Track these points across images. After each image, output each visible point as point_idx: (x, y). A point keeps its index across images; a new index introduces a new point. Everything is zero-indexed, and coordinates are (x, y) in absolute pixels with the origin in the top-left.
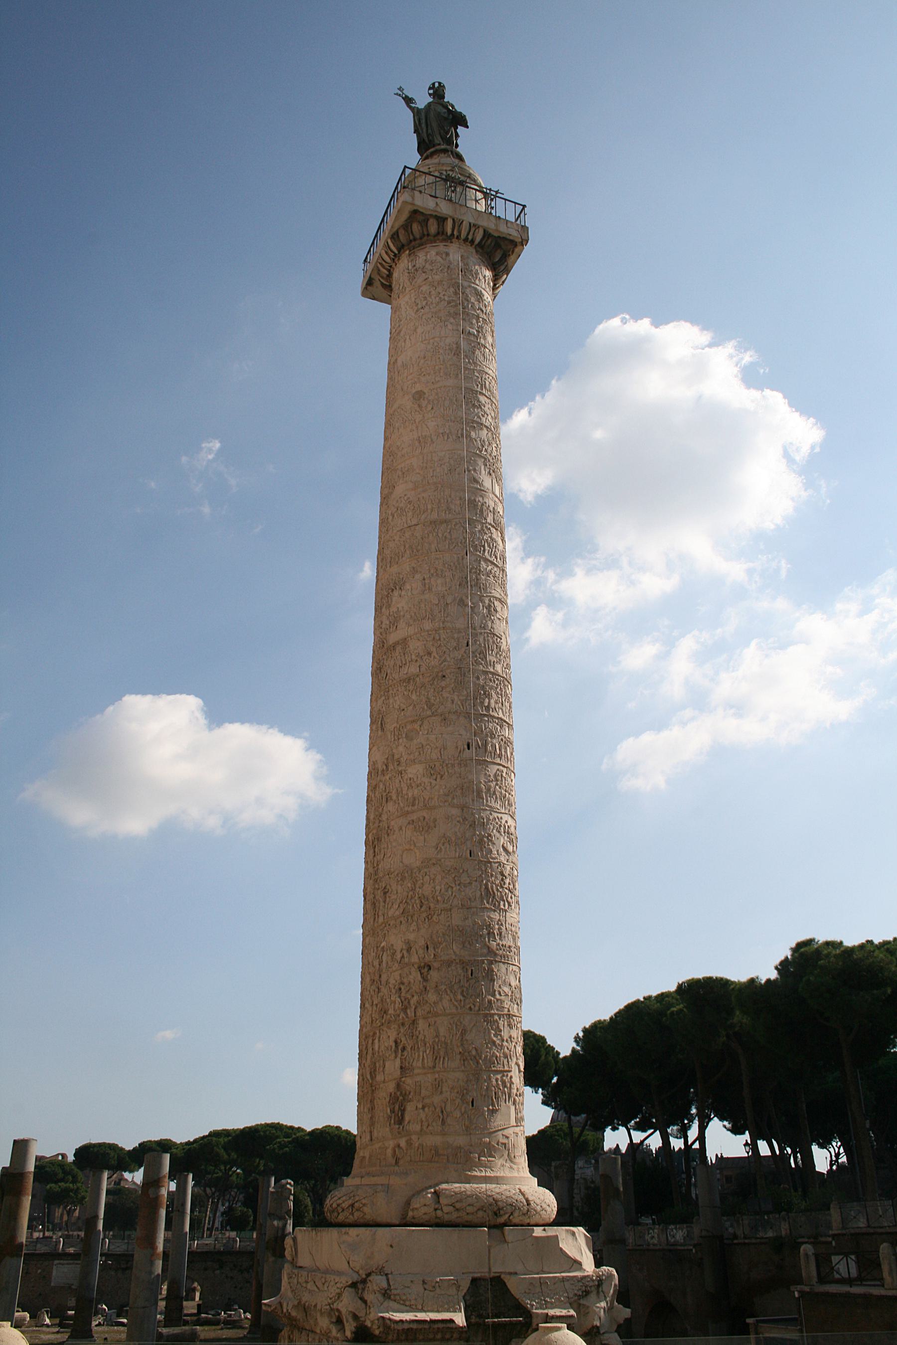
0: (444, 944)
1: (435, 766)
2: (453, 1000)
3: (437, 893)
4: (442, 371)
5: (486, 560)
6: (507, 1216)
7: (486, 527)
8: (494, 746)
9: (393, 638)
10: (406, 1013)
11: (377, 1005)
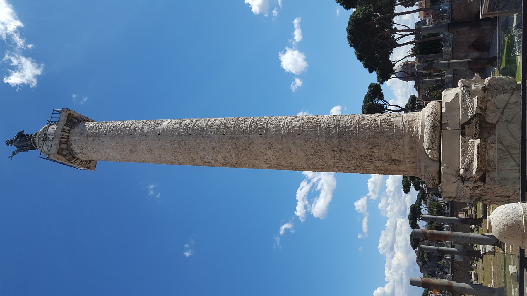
0: (332, 144)
2: (353, 141)
3: (314, 147)
4: (121, 143)
5: (193, 127)
6: (437, 122)
7: (181, 127)
8: (260, 125)
9: (222, 161)
10: (358, 159)
11: (355, 168)
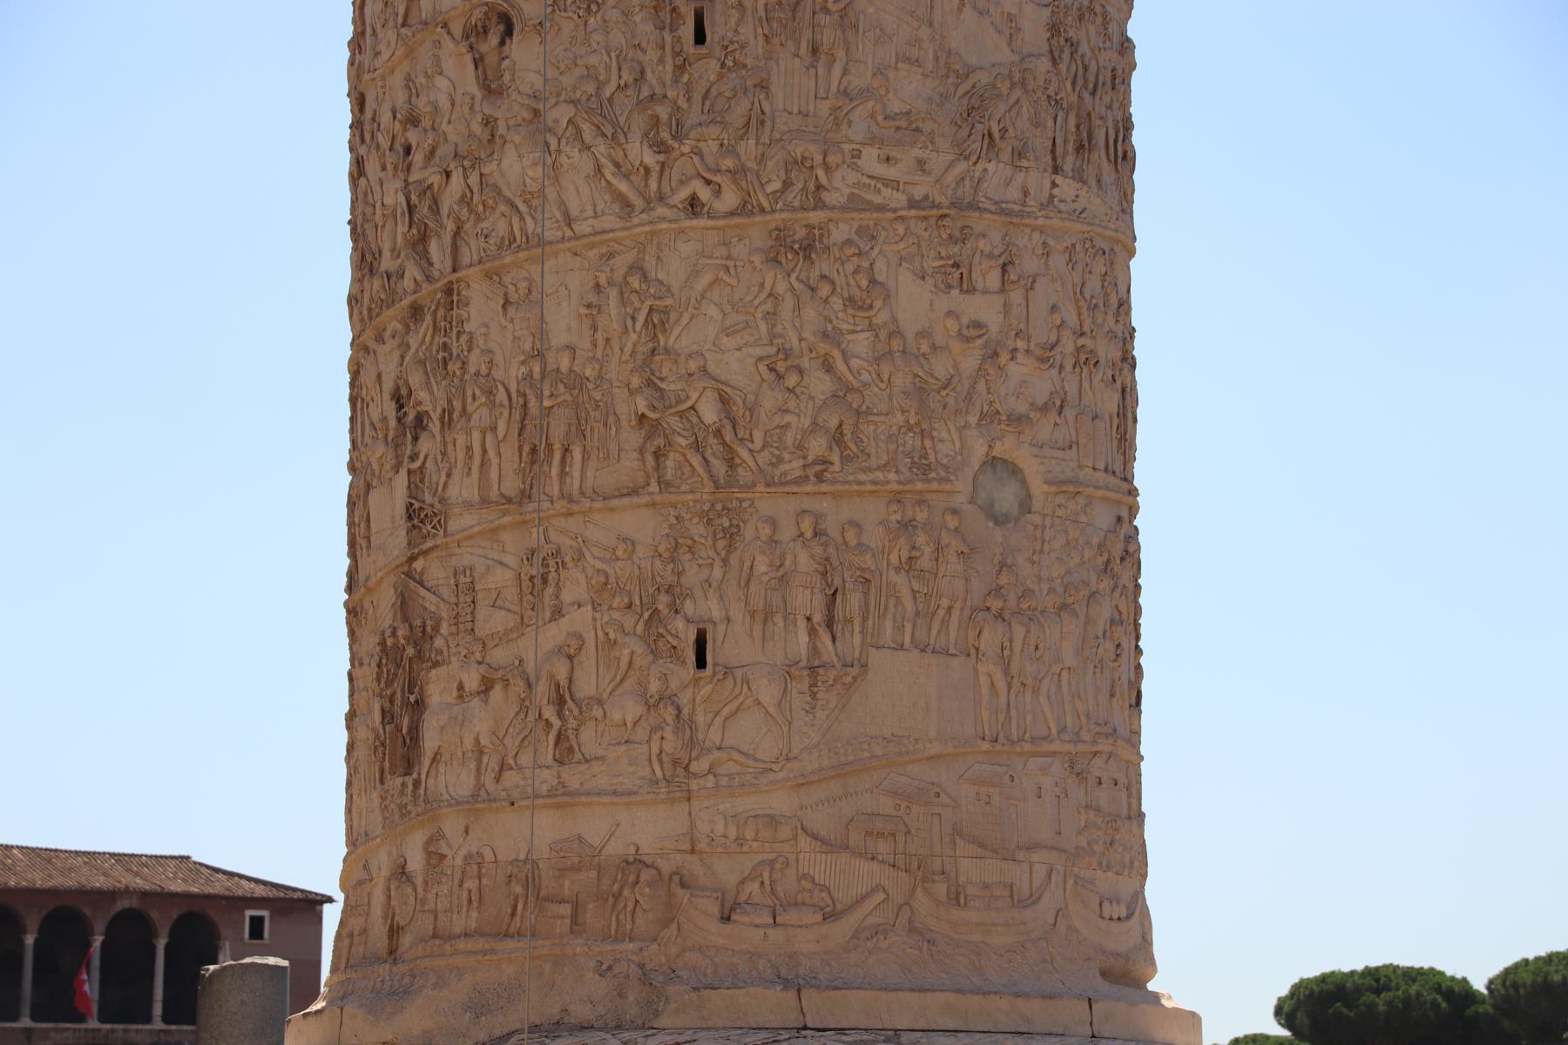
2: (609, 170)
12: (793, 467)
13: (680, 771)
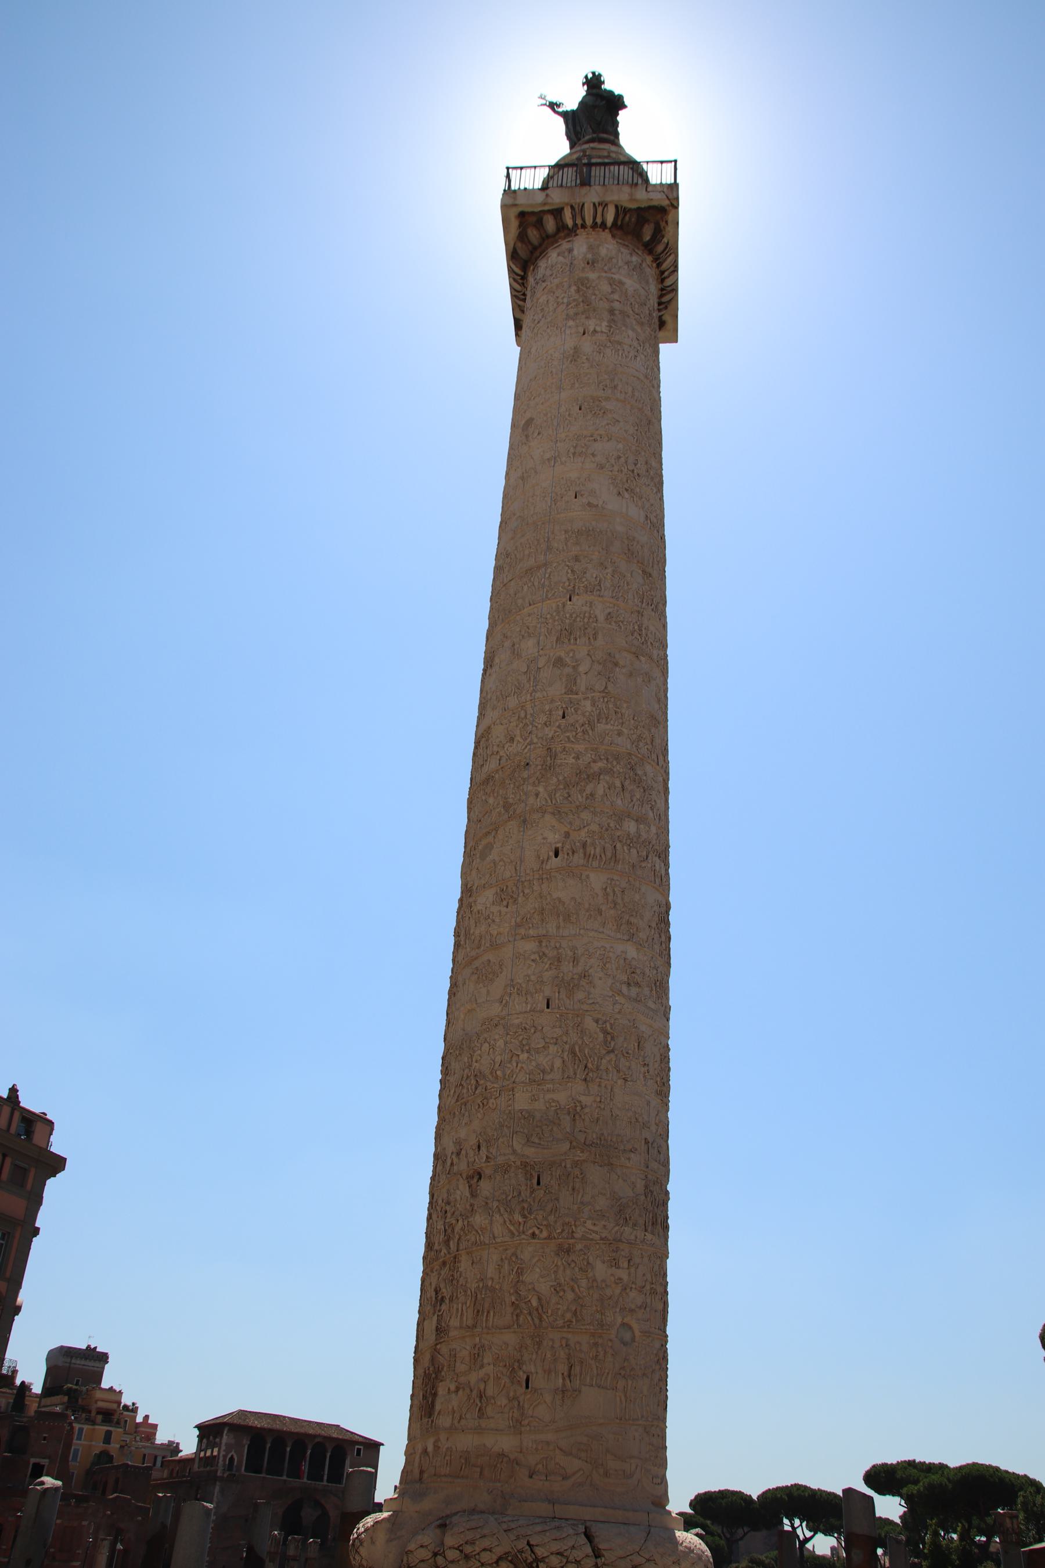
1: (507, 886)
2: (508, 1223)
12: (560, 1322)
13: (518, 1424)
